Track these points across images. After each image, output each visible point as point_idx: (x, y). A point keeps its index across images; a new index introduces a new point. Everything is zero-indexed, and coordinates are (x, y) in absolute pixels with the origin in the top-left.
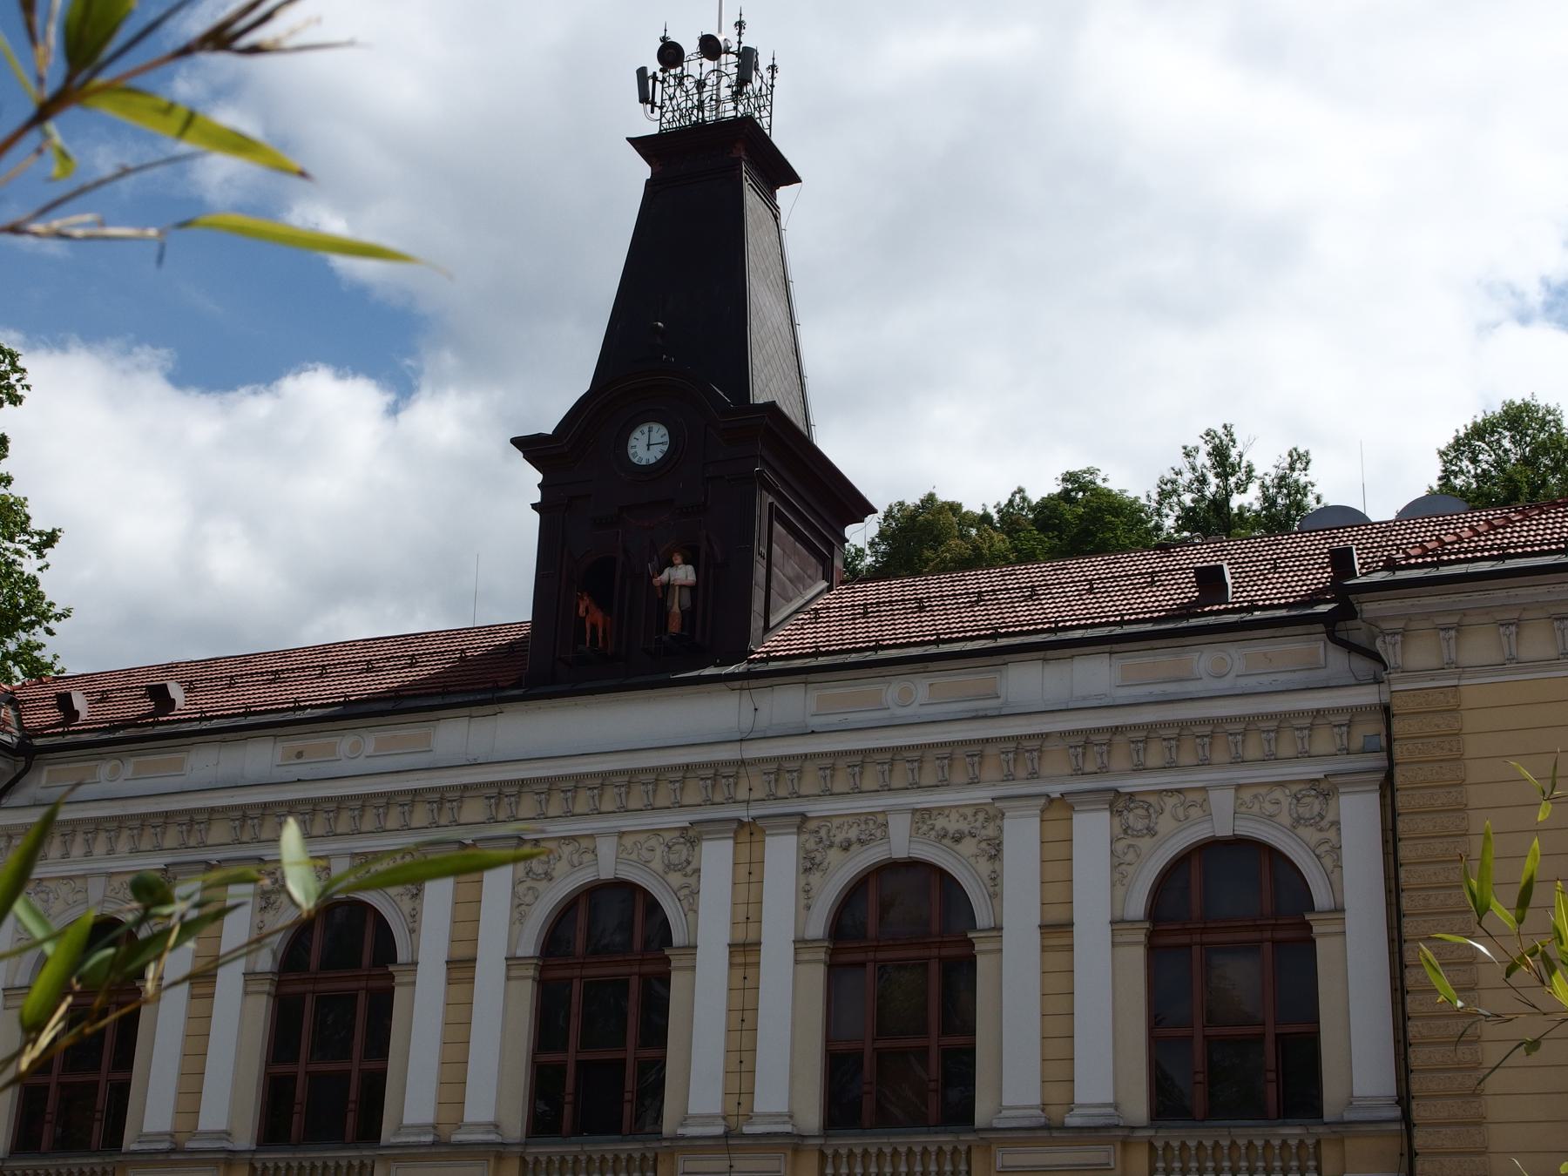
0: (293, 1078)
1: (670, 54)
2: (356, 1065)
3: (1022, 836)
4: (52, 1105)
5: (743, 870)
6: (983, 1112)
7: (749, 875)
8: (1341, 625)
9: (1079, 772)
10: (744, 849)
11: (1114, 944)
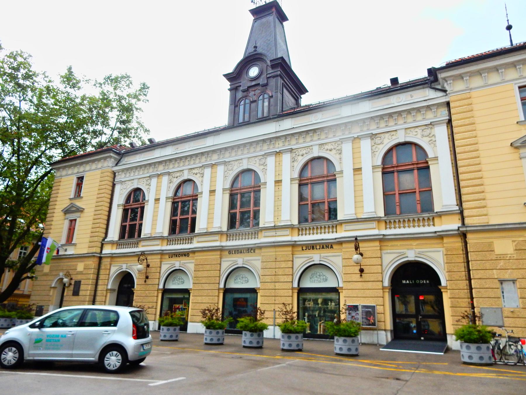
0: (176, 220)
2: (190, 216)
3: (347, 148)
4: (127, 229)
5: (278, 163)
8: (433, 84)
9: (362, 131)
10: (278, 158)
11: (373, 172)
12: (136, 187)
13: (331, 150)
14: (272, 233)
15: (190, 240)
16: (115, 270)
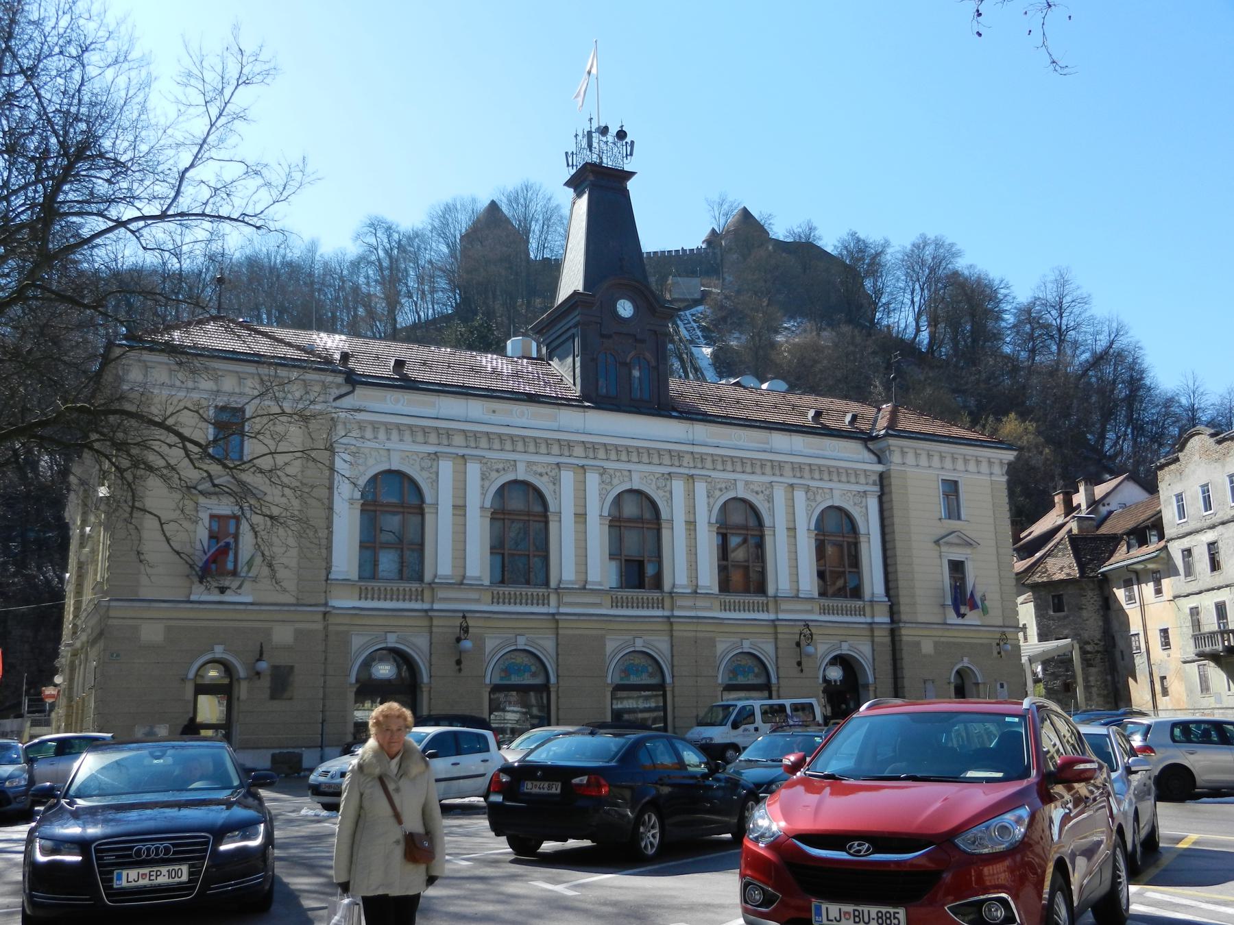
1: (604, 131)
3: (779, 495)
6: (771, 590)
7: (691, 495)
12: (395, 466)
13: (757, 493)
14: (689, 603)
15: (545, 601)
16: (360, 644)
